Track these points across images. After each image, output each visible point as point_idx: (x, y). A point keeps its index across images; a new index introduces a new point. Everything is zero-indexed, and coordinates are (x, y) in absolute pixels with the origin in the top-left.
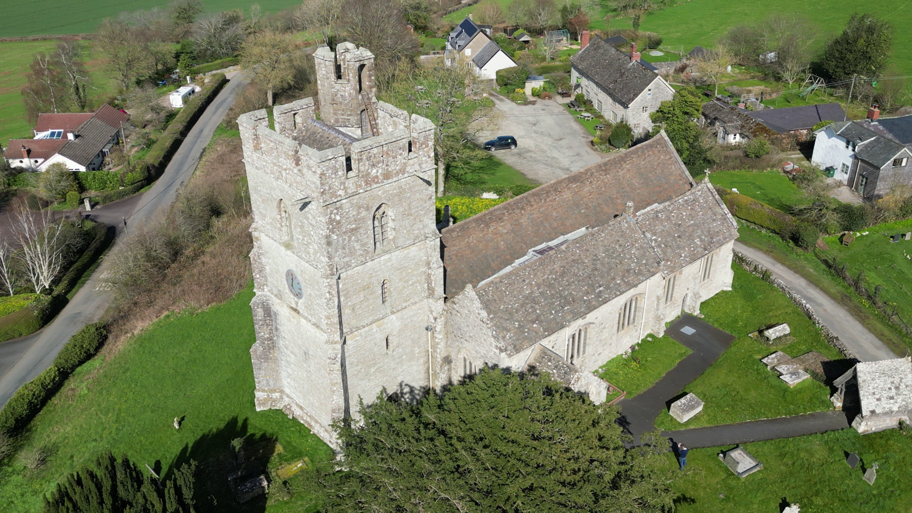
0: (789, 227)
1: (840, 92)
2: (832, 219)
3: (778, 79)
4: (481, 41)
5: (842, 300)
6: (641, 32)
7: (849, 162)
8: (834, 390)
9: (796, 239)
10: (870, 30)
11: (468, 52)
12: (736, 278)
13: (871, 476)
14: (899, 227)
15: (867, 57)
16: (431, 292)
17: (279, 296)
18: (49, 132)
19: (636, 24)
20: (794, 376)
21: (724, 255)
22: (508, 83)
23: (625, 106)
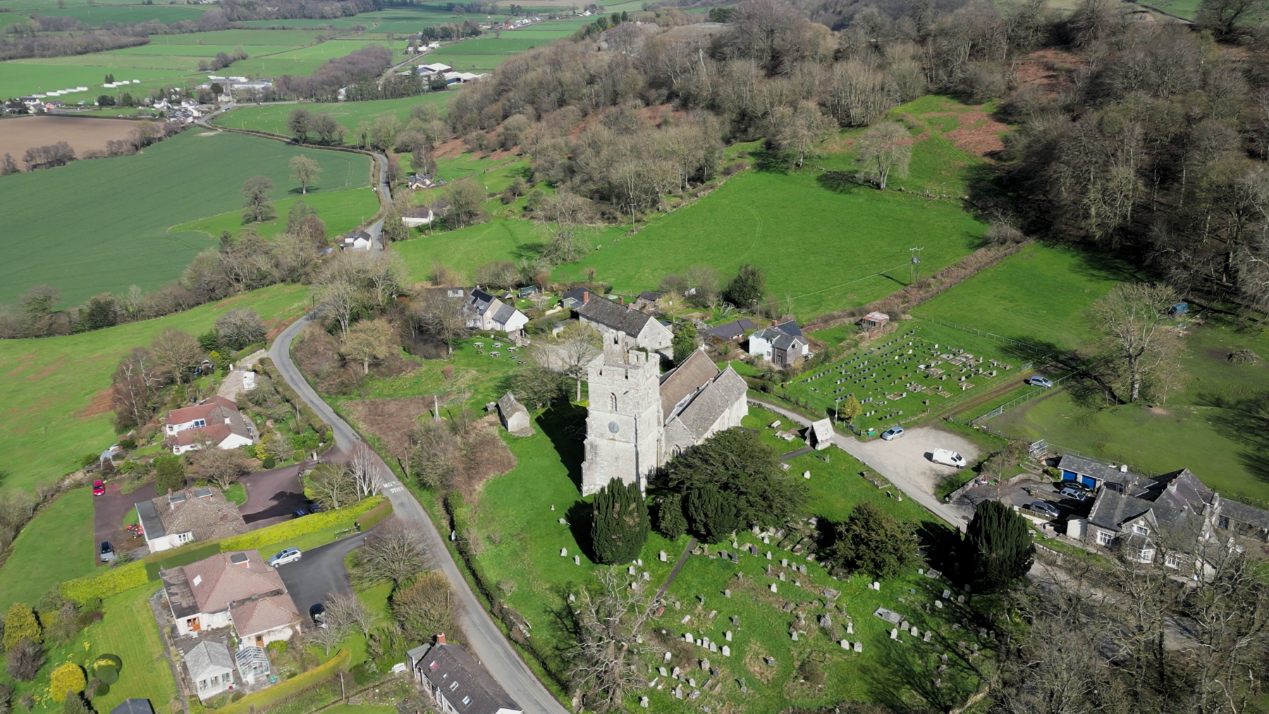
0: (760, 385)
1: (744, 311)
2: (777, 377)
3: (706, 307)
4: (497, 304)
5: (793, 411)
6: (594, 283)
7: (770, 350)
8: (805, 438)
9: (764, 389)
10: (753, 274)
11: (489, 314)
12: (750, 408)
13: (828, 460)
14: (804, 377)
15: (754, 289)
16: (659, 423)
17: (602, 436)
18: (193, 422)
19: (591, 278)
20: (790, 437)
21: (744, 398)
22: (535, 330)
23: (635, 336)
